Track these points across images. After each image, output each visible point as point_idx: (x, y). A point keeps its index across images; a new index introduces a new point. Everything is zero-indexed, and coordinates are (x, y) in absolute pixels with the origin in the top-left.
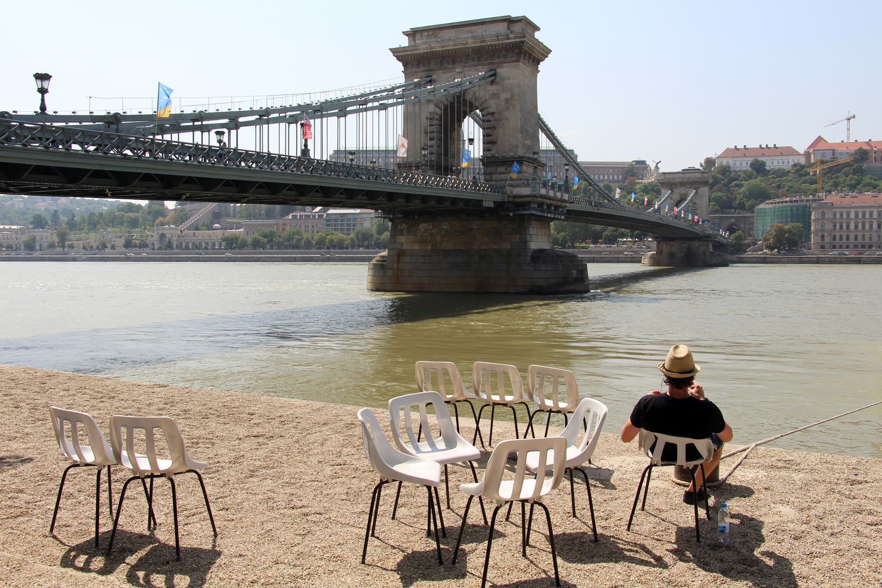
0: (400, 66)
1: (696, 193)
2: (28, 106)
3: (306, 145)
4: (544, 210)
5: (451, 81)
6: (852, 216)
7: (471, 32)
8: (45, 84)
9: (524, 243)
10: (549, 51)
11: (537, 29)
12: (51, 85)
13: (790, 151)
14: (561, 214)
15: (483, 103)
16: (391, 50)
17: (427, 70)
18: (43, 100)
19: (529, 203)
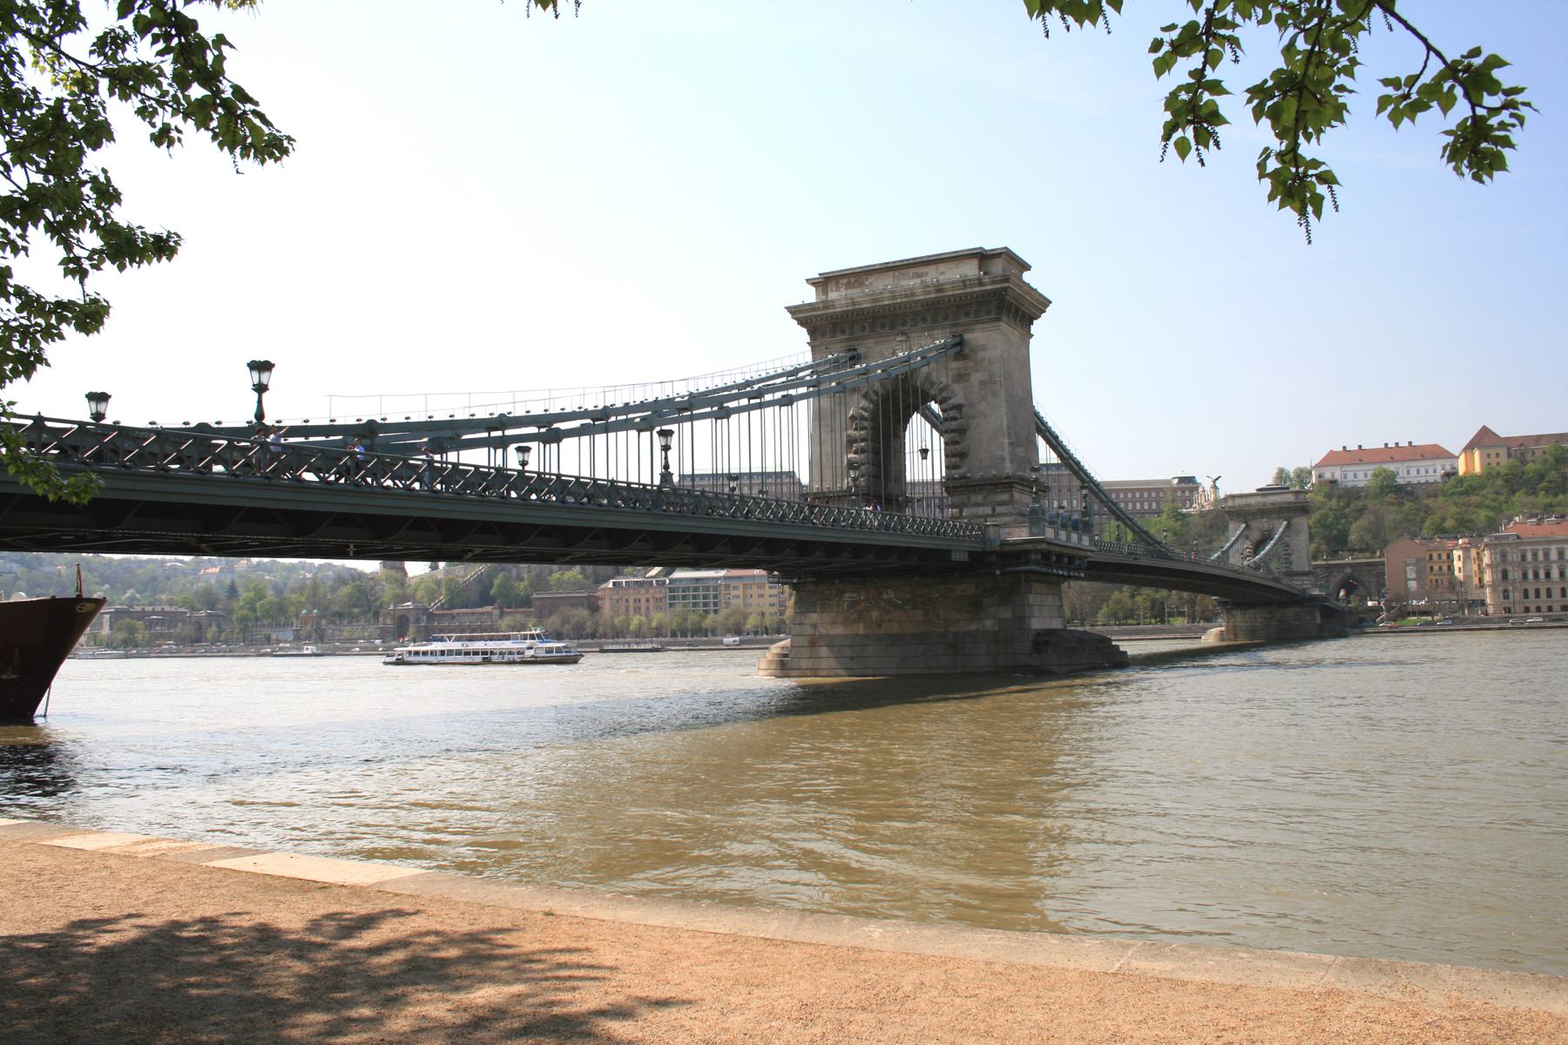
0: (803, 335)
1: (1288, 526)
2: (238, 414)
3: (666, 467)
4: (1053, 565)
6: (1554, 555)
8: (265, 378)
9: (1020, 620)
10: (1047, 303)
11: (1028, 268)
12: (272, 379)
13: (1437, 453)
14: (1079, 569)
15: (942, 390)
16: (789, 309)
18: (260, 402)
19: (1027, 552)
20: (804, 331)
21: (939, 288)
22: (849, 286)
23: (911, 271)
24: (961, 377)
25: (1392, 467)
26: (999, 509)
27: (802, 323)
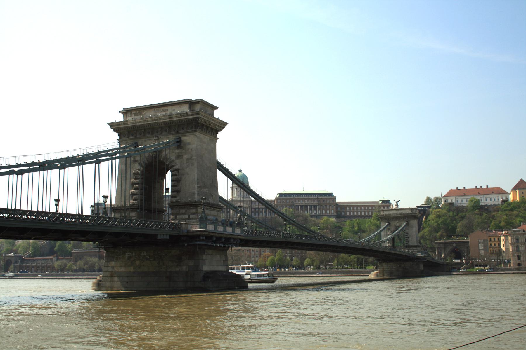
0: (116, 136)
1: (408, 224)
4: (221, 243)
7: (164, 111)
11: (216, 108)
13: (499, 191)
16: (109, 124)
17: (134, 139)
20: (117, 134)
22: (136, 114)
23: (162, 109)
24: (179, 157)
25: (479, 197)
26: (191, 216)
27: (115, 130)
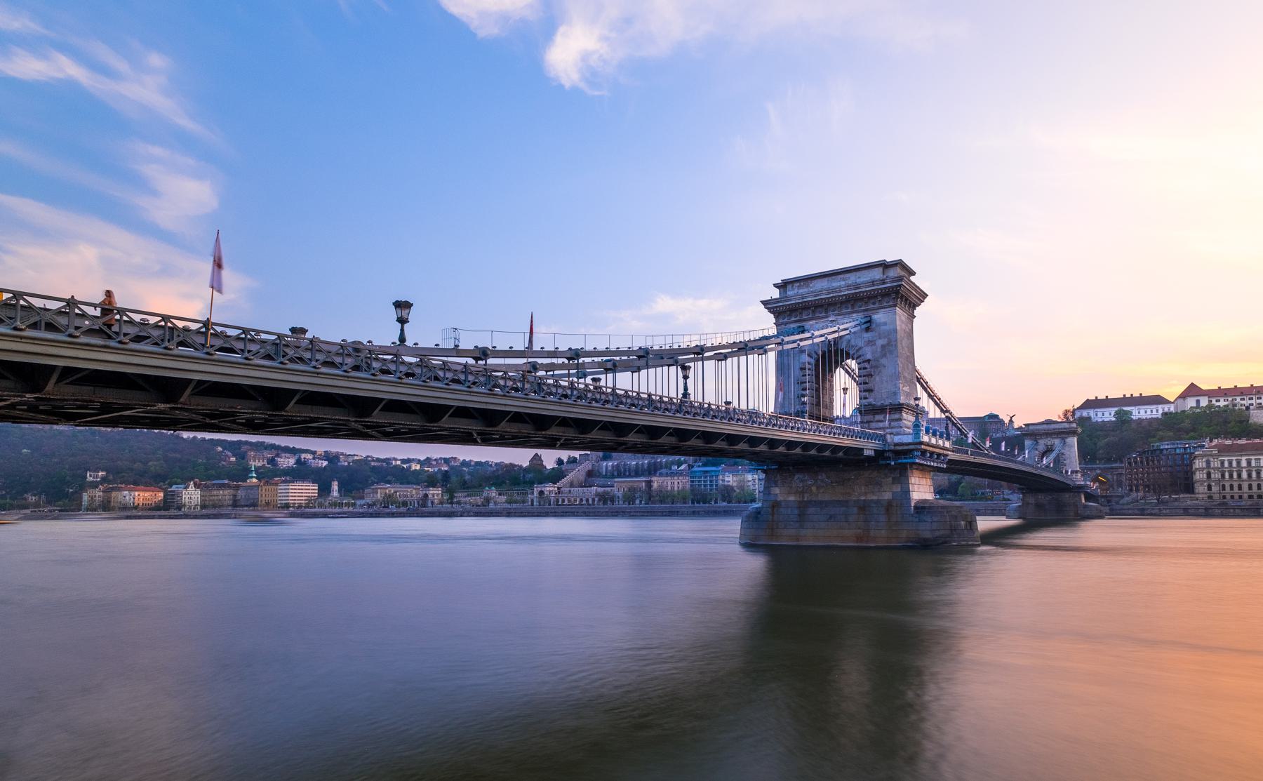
0: (771, 318)
2: (383, 334)
5: (822, 332)
8: (405, 312)
9: (907, 493)
10: (925, 295)
11: (913, 273)
12: (413, 315)
13: (1158, 400)
18: (402, 330)
21: (856, 286)
